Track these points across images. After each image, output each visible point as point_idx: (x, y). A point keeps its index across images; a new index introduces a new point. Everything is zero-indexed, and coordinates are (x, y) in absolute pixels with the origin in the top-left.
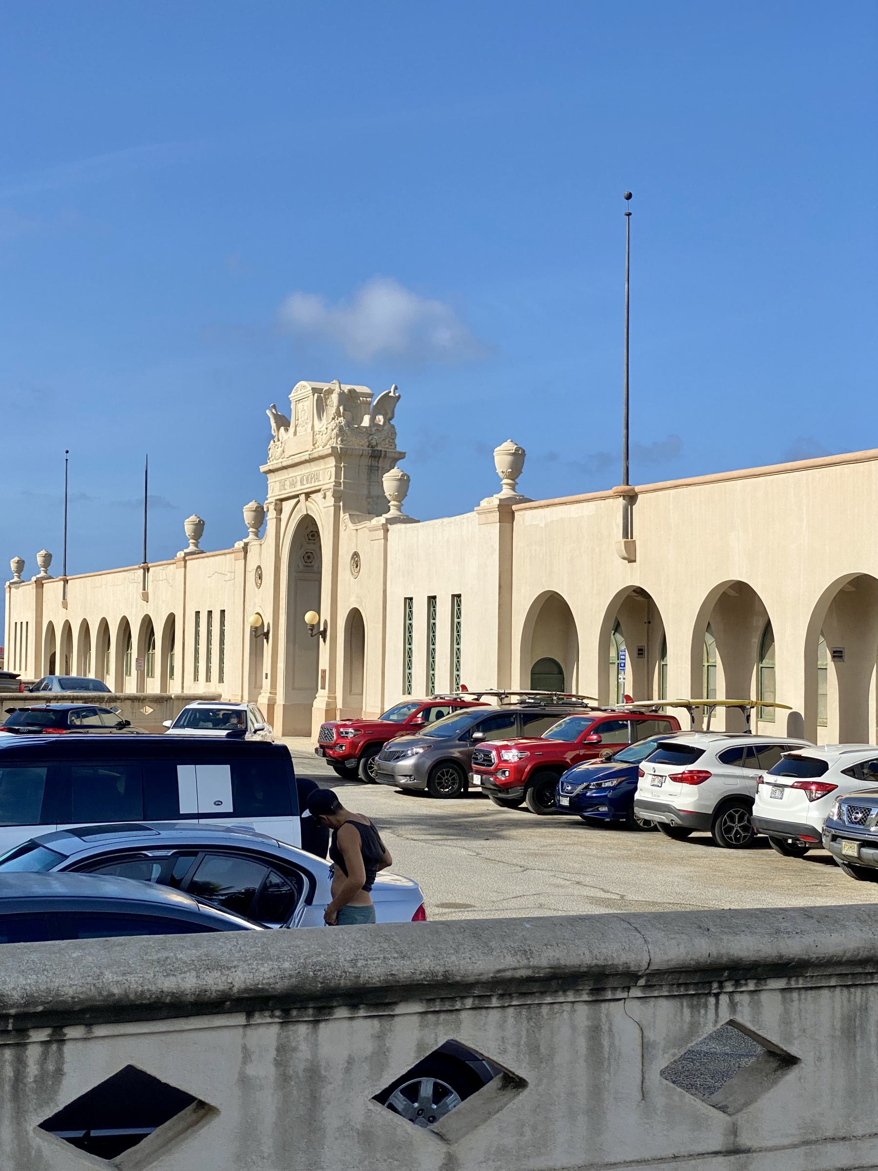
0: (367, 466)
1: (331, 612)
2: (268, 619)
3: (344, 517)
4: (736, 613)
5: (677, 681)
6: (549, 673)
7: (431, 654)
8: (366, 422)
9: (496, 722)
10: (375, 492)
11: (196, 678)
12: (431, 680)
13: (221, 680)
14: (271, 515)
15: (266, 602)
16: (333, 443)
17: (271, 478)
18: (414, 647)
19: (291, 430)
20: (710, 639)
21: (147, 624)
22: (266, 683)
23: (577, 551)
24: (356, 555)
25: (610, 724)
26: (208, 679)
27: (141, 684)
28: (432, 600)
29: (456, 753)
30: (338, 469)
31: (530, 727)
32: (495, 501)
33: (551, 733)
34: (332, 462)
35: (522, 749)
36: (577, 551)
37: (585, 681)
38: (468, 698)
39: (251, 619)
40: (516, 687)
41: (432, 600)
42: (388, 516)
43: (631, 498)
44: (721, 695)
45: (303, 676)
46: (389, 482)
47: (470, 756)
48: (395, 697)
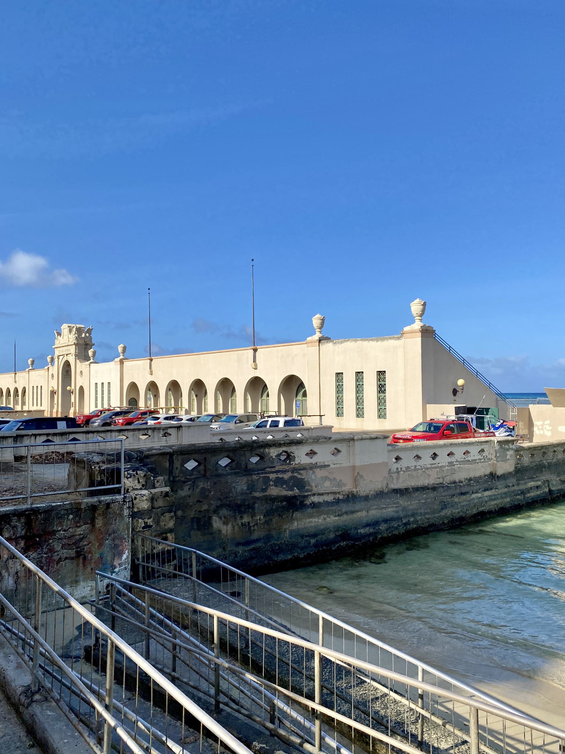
0: (84, 347)
1: (75, 386)
2: (56, 388)
3: (78, 361)
4: (174, 386)
5: (162, 402)
6: (133, 402)
7: (103, 398)
8: (83, 335)
9: (117, 414)
10: (86, 354)
11: (33, 405)
12: (103, 404)
13: (41, 405)
14: (56, 360)
15: (55, 384)
16: (74, 341)
17: (56, 350)
18: (98, 396)
19: (62, 336)
20: (193, 392)
21: (16, 390)
22: (56, 406)
23: (139, 372)
24: (81, 371)
25: (144, 413)
26: (37, 405)
28: (103, 384)
29: (108, 421)
30: (76, 348)
31: (126, 415)
33: (130, 416)
34: (74, 346)
35: (123, 419)
36: (139, 372)
37: (142, 404)
38: (111, 408)
39: (51, 389)
40: (125, 405)
41: (103, 384)
42: (90, 361)
43: (151, 360)
44: (173, 406)
45: (66, 403)
46: (90, 353)
47: (111, 422)
48: (93, 409)
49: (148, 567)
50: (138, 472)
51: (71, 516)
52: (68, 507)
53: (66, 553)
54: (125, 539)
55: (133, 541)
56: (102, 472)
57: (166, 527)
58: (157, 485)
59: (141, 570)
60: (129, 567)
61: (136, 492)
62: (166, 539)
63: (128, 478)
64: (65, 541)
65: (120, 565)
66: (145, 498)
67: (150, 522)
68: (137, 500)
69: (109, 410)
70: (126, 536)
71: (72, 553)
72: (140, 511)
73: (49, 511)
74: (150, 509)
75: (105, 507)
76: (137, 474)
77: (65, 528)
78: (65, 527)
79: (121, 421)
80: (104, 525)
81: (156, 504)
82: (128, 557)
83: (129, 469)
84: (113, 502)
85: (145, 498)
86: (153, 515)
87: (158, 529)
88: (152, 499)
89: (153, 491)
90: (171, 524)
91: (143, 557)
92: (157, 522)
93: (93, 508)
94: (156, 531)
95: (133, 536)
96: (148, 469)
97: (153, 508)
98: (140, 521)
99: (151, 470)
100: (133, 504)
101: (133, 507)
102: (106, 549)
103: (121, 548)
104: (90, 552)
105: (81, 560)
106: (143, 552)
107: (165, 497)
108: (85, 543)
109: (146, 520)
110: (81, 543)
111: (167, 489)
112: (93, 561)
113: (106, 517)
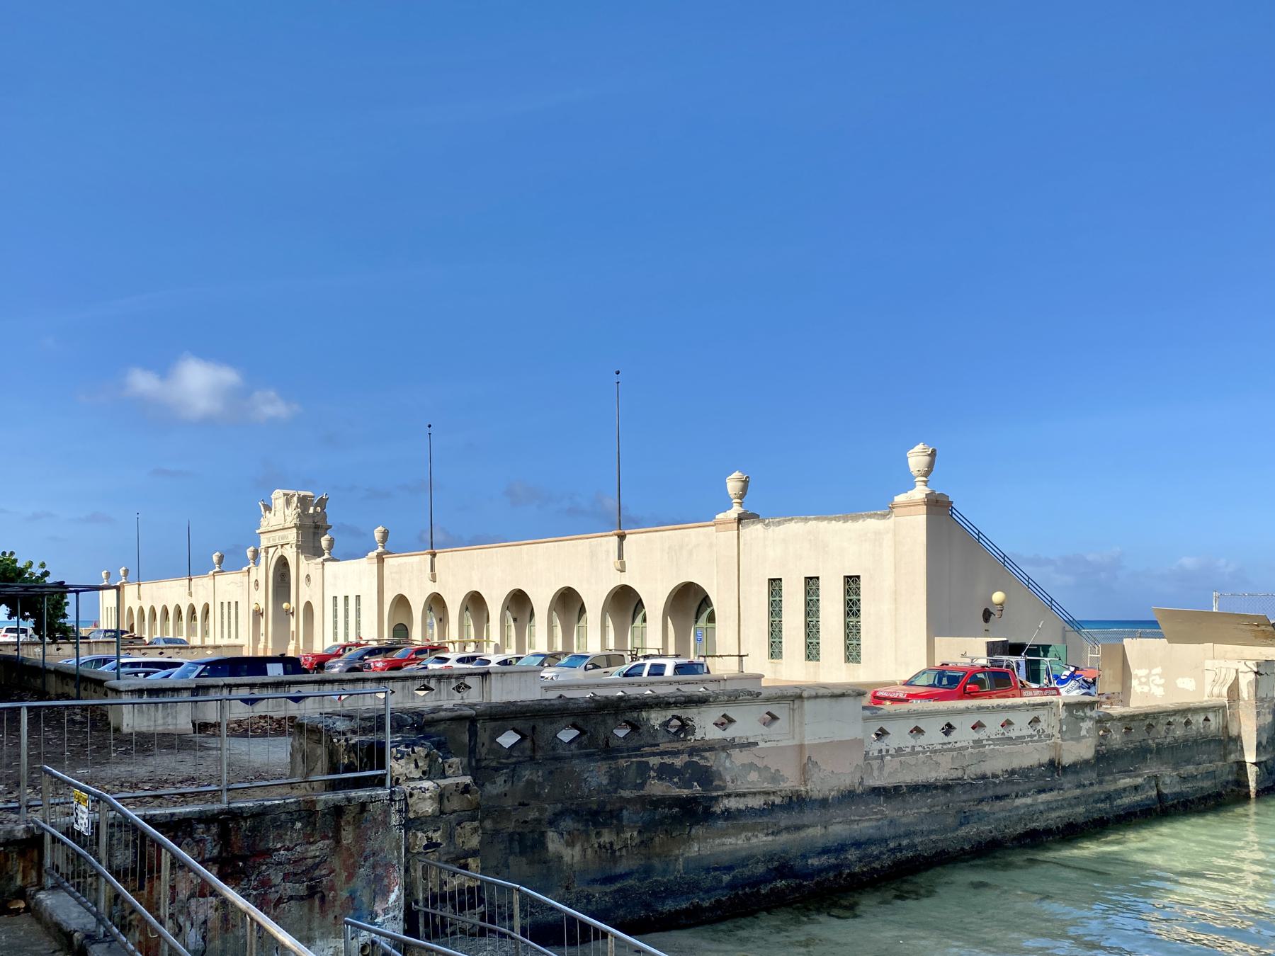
5: (453, 632)
6: (402, 630)
7: (346, 623)
9: (373, 652)
12: (346, 635)
22: (262, 638)
23: (410, 575)
25: (422, 651)
27: (203, 640)
28: (346, 597)
32: (374, 554)
33: (397, 655)
40: (386, 637)
41: (346, 597)
43: (434, 555)
48: (329, 643)
49: (434, 916)
50: (416, 749)
51: (298, 825)
52: (294, 807)
53: (289, 888)
54: (393, 866)
55: (407, 870)
56: (351, 749)
57: (466, 848)
58: (449, 772)
59: (421, 920)
60: (401, 916)
61: (412, 784)
62: (465, 867)
63: (397, 759)
64: (290, 868)
65: (386, 911)
66: (428, 795)
67: (437, 837)
68: (415, 798)
69: (358, 645)
70: (395, 862)
71: (302, 889)
72: (418, 818)
73: (260, 814)
74: (437, 813)
75: (358, 809)
76: (413, 751)
77: (289, 846)
78: (287, 843)
79: (379, 665)
80: (357, 842)
81: (448, 806)
82: (398, 898)
83: (400, 743)
84: (373, 800)
85: (428, 795)
86: (441, 825)
87: (452, 849)
88: (441, 797)
89: (443, 782)
90: (474, 842)
91: (426, 899)
92: (450, 837)
93: (337, 811)
94: (449, 853)
95: (408, 862)
96: (433, 743)
97: (442, 812)
98: (420, 834)
99: (439, 746)
100: (407, 805)
101: (407, 811)
102: (358, 883)
103: (386, 881)
104: (332, 888)
105: (317, 902)
106: (425, 890)
107: (463, 793)
108: (323, 872)
109: (430, 834)
110: (317, 873)
111: (468, 780)
112: (338, 903)
113: (359, 827)
